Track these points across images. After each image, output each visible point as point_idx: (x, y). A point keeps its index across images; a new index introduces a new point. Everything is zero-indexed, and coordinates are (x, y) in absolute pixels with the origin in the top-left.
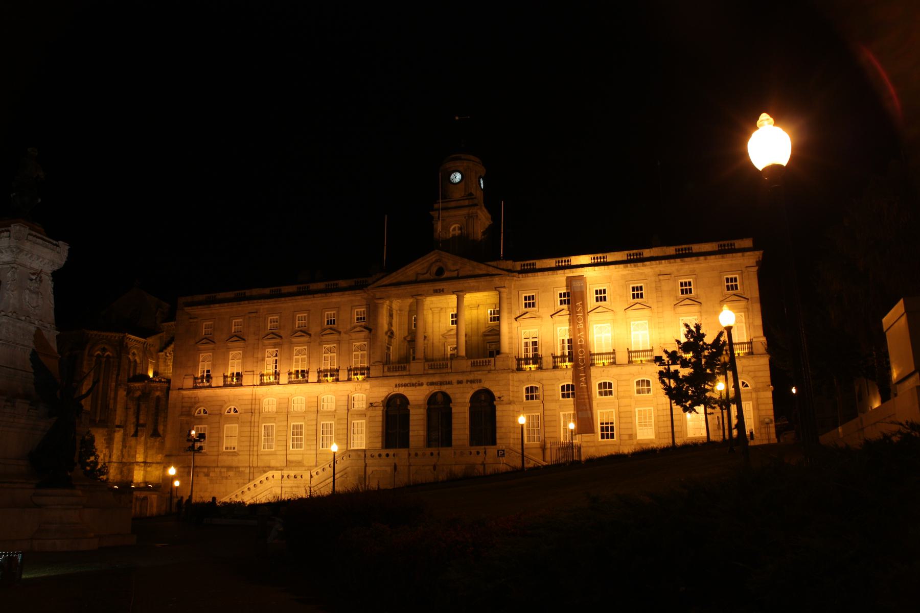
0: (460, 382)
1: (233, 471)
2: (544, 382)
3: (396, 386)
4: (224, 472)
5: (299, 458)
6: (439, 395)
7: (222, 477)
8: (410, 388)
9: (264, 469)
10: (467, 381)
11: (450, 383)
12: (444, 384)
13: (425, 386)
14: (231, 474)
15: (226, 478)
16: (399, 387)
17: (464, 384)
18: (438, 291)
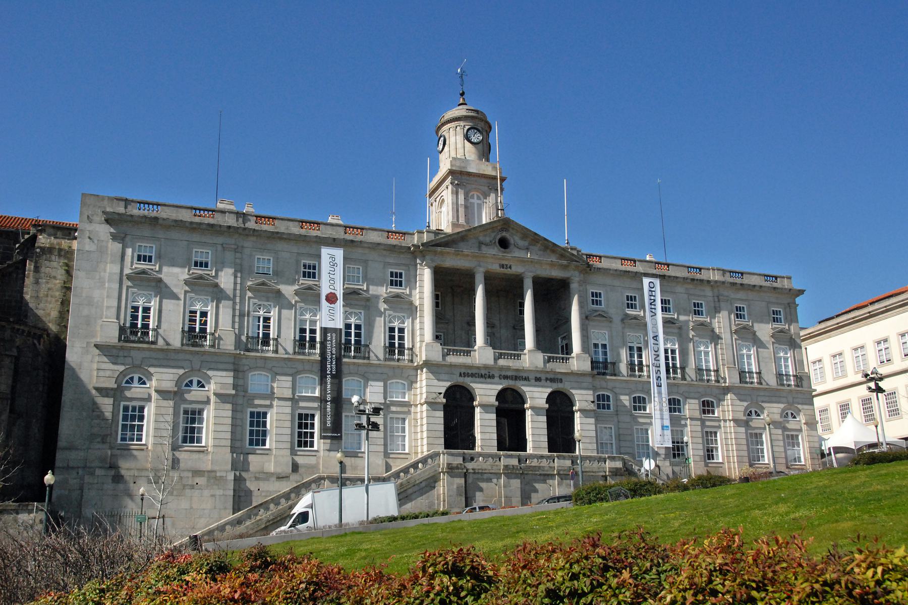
0: (538, 379)
1: (203, 476)
2: (617, 390)
3: (460, 375)
4: (188, 477)
5: (312, 460)
6: (509, 392)
7: (184, 486)
8: (478, 380)
9: (257, 475)
10: (547, 379)
11: (526, 379)
12: (520, 380)
13: (497, 379)
14: (202, 481)
15: (192, 487)
16: (465, 376)
17: (543, 382)
18: (505, 266)
